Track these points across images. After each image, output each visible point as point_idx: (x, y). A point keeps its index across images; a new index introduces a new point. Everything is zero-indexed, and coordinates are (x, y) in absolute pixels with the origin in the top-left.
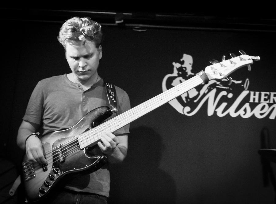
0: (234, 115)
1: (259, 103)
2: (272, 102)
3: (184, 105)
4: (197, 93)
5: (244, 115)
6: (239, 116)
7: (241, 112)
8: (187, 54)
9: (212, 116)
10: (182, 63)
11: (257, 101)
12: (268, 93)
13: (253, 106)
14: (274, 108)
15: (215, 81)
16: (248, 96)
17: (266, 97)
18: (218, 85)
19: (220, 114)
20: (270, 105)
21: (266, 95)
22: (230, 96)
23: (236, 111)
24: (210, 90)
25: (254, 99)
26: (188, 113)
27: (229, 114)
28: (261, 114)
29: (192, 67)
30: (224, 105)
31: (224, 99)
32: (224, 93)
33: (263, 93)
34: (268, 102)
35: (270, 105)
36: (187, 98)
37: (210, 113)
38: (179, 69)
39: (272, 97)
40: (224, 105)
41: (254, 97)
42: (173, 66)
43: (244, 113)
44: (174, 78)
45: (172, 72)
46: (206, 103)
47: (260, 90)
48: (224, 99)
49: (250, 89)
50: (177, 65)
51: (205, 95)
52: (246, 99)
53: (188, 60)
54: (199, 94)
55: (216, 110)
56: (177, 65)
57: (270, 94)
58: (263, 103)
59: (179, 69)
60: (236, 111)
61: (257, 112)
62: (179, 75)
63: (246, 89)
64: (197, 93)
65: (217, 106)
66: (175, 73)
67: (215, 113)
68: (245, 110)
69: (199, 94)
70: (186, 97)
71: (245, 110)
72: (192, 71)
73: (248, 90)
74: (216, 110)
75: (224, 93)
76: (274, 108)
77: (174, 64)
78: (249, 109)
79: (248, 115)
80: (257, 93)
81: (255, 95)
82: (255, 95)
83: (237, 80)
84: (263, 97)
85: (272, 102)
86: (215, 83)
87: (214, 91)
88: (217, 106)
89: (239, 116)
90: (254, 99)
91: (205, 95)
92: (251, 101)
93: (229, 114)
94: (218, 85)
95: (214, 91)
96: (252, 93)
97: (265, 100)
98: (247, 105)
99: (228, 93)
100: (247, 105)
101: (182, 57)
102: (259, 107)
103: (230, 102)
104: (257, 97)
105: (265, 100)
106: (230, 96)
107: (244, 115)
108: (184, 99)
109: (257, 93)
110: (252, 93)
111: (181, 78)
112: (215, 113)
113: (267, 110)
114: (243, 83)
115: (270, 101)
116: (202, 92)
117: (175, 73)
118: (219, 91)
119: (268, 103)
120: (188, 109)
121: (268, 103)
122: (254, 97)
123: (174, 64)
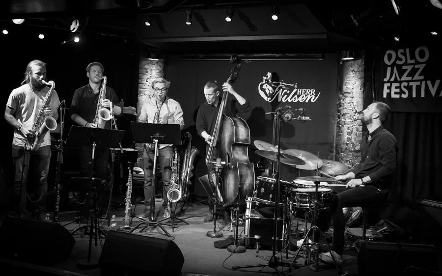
0: (290, 101)
1: (301, 95)
3: (268, 97)
7: (293, 99)
10: (267, 77)
13: (299, 96)
16: (297, 91)
19: (284, 101)
20: (306, 95)
24: (279, 89)
30: (286, 96)
31: (286, 93)
32: (286, 91)
33: (303, 90)
35: (306, 95)
36: (269, 93)
37: (279, 100)
39: (307, 92)
40: (286, 96)
44: (264, 84)
45: (263, 82)
47: (302, 89)
50: (265, 78)
51: (277, 92)
52: (296, 93)
53: (269, 74)
56: (265, 78)
58: (303, 95)
61: (300, 99)
66: (264, 82)
68: (295, 98)
71: (295, 98)
75: (286, 91)
78: (297, 98)
79: (296, 101)
80: (301, 90)
84: (303, 92)
87: (281, 90)
91: (277, 92)
92: (298, 94)
95: (281, 90)
96: (298, 90)
97: (304, 93)
98: (296, 96)
100: (296, 96)
102: (301, 96)
103: (288, 95)
105: (304, 93)
106: (288, 92)
109: (301, 90)
110: (298, 90)
111: (267, 84)
112: (282, 100)
113: (305, 98)
114: (294, 86)
117: (264, 82)
118: (283, 90)
120: (270, 98)
122: (299, 92)
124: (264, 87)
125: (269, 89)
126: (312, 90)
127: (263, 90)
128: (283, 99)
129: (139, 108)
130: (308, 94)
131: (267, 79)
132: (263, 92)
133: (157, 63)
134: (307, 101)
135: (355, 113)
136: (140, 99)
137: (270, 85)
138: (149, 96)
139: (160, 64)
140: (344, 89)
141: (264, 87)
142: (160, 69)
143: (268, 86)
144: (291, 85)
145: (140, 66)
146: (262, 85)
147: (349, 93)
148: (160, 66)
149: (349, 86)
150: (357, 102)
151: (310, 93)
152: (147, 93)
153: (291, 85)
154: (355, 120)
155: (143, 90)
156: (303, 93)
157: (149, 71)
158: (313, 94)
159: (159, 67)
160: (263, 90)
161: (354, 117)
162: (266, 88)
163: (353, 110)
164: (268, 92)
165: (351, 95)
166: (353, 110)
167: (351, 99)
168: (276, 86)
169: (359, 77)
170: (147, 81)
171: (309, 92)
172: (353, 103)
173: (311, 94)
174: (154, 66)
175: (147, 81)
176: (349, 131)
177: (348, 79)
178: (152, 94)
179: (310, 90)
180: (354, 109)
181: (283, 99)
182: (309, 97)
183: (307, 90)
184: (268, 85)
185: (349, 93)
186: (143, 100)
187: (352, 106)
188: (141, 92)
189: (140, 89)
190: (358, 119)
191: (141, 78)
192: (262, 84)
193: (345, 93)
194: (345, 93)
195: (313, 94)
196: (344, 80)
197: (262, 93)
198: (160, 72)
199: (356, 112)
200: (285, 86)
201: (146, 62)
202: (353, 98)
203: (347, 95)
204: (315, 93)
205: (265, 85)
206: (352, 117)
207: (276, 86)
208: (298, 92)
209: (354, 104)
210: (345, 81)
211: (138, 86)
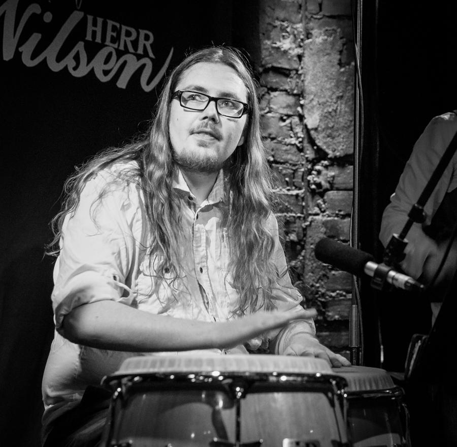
0: (55, 67)
1: (102, 45)
2: (122, 48)
5: (75, 69)
6: (66, 68)
7: (69, 61)
9: (10, 61)
11: (98, 40)
12: (118, 25)
13: (92, 50)
14: (125, 63)
16: (82, 25)
17: (115, 34)
20: (120, 54)
21: (114, 29)
23: (59, 59)
25: (94, 33)
27: (44, 62)
28: (106, 73)
30: (35, 38)
31: (34, 24)
32: (35, 9)
33: (110, 23)
34: (116, 46)
39: (123, 37)
40: (35, 38)
41: (94, 29)
43: (74, 64)
47: (106, 18)
48: (34, 24)
49: (86, 10)
52: (78, 34)
55: (20, 49)
57: (121, 27)
58: (110, 48)
60: (59, 59)
63: (79, 8)
65: (22, 42)
67: (18, 55)
68: (77, 58)
71: (77, 58)
73: (80, 10)
74: (20, 49)
75: (35, 9)
76: (125, 63)
81: (95, 24)
82: (95, 24)
84: (109, 33)
85: (122, 48)
88: (22, 42)
90: (94, 33)
92: (89, 37)
93: (45, 60)
96: (90, 18)
98: (80, 47)
100: (80, 47)
102: (102, 54)
104: (99, 30)
106: (48, 17)
107: (75, 69)
109: (100, 21)
112: (18, 55)
113: (114, 65)
115: (119, 46)
119: (115, 49)
121: (115, 49)
126: (143, 33)
128: (27, 49)
130: (126, 51)
134: (122, 83)
135: (314, 162)
140: (264, 53)
147: (284, 73)
149: (285, 44)
150: (325, 117)
151: (135, 44)
154: (313, 193)
156: (108, 42)
158: (146, 54)
161: (309, 178)
163: (301, 150)
165: (289, 84)
166: (301, 150)
167: (291, 100)
169: (326, 11)
171: (128, 40)
172: (301, 117)
173: (140, 51)
176: (293, 237)
177: (282, 14)
179: (133, 30)
180: (306, 144)
181: (27, 49)
182: (133, 65)
183: (124, 28)
185: (284, 73)
187: (298, 129)
190: (332, 189)
193: (267, 71)
194: (267, 71)
195: (146, 54)
196: (264, 11)
199: (321, 155)
202: (300, 95)
203: (273, 79)
204: (151, 45)
206: (298, 180)
208: (90, 28)
209: (312, 121)
210: (268, 20)
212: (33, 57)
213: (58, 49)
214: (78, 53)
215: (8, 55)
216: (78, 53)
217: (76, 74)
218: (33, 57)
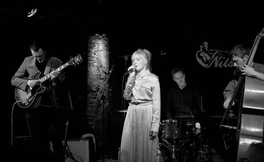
0: (226, 66)
3: (205, 63)
4: (210, 58)
6: (228, 66)
7: (229, 65)
8: (205, 41)
9: (217, 67)
10: (204, 45)
15: (218, 52)
18: (219, 54)
19: (220, 66)
22: (224, 58)
23: (227, 65)
24: (215, 56)
26: (207, 67)
27: (224, 65)
29: (208, 47)
30: (222, 62)
31: (222, 60)
32: (221, 57)
36: (206, 60)
37: (216, 66)
38: (202, 49)
40: (222, 62)
42: (200, 47)
43: (230, 65)
44: (201, 52)
46: (214, 62)
50: (202, 47)
51: (213, 58)
53: (206, 44)
54: (211, 58)
56: (202, 47)
59: (202, 49)
62: (203, 51)
64: (210, 58)
65: (219, 63)
66: (201, 50)
67: (218, 66)
68: (231, 64)
69: (211, 58)
70: (206, 60)
71: (231, 64)
72: (208, 49)
75: (221, 57)
77: (200, 46)
78: (232, 63)
83: (227, 51)
86: (218, 53)
87: (218, 56)
88: (219, 63)
89: (228, 66)
91: (213, 58)
93: (224, 65)
94: (219, 54)
95: (218, 56)
99: (223, 57)
101: (203, 43)
106: (224, 58)
108: (205, 61)
111: (203, 52)
112: (218, 66)
116: (212, 58)
117: (201, 50)
118: (219, 57)
120: (207, 65)
123: (200, 46)
124: (201, 55)
125: (206, 57)
127: (201, 58)
129: (89, 79)
131: (203, 48)
132: (200, 60)
133: (103, 37)
136: (89, 70)
137: (207, 52)
138: (97, 67)
139: (105, 38)
141: (201, 55)
142: (106, 43)
143: (206, 54)
144: (227, 52)
145: (89, 42)
146: (199, 53)
148: (106, 40)
152: (95, 64)
153: (227, 52)
155: (92, 62)
157: (96, 45)
159: (105, 41)
160: (201, 58)
162: (203, 55)
164: (205, 59)
168: (212, 54)
170: (95, 54)
174: (101, 40)
175: (95, 54)
178: (100, 65)
184: (204, 53)
186: (93, 70)
188: (90, 64)
189: (89, 62)
191: (90, 52)
192: (199, 52)
197: (199, 61)
198: (106, 46)
200: (221, 53)
201: (94, 37)
205: (202, 53)
207: (212, 54)
211: (88, 58)
212: (221, 66)
213: (221, 64)
214: (231, 63)
215: (216, 66)
216: (231, 63)
217: (231, 66)
218: (221, 66)
